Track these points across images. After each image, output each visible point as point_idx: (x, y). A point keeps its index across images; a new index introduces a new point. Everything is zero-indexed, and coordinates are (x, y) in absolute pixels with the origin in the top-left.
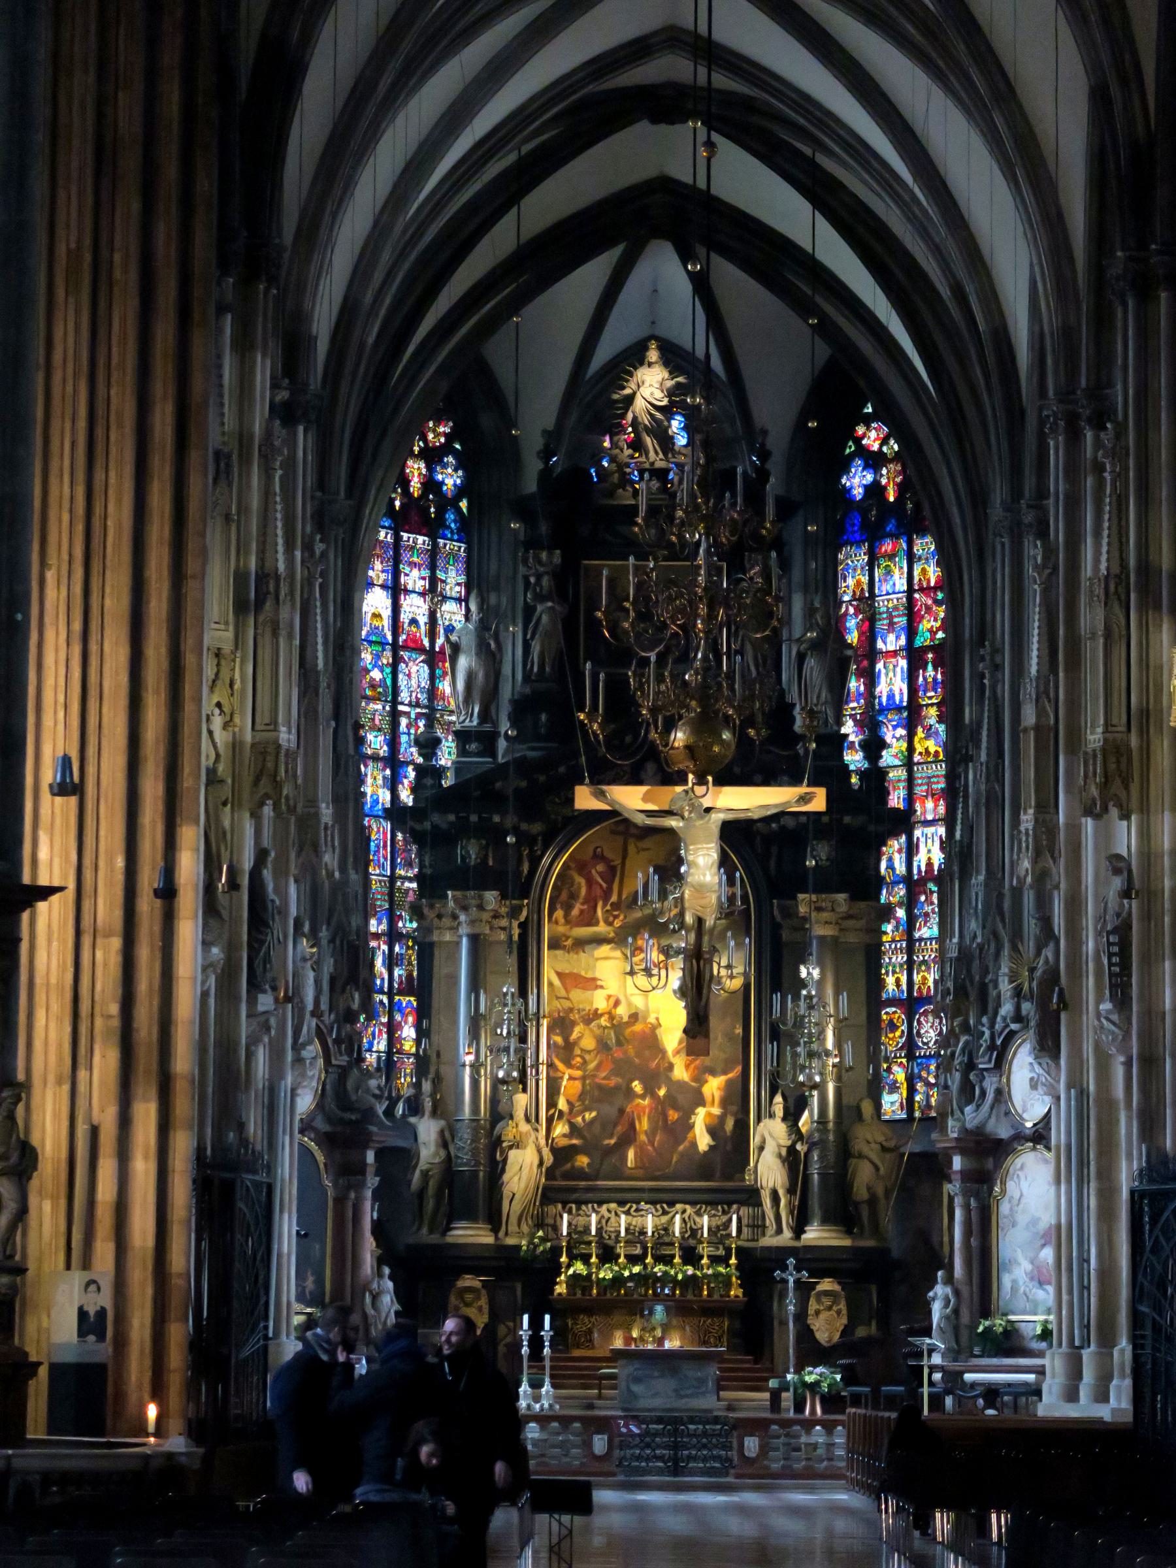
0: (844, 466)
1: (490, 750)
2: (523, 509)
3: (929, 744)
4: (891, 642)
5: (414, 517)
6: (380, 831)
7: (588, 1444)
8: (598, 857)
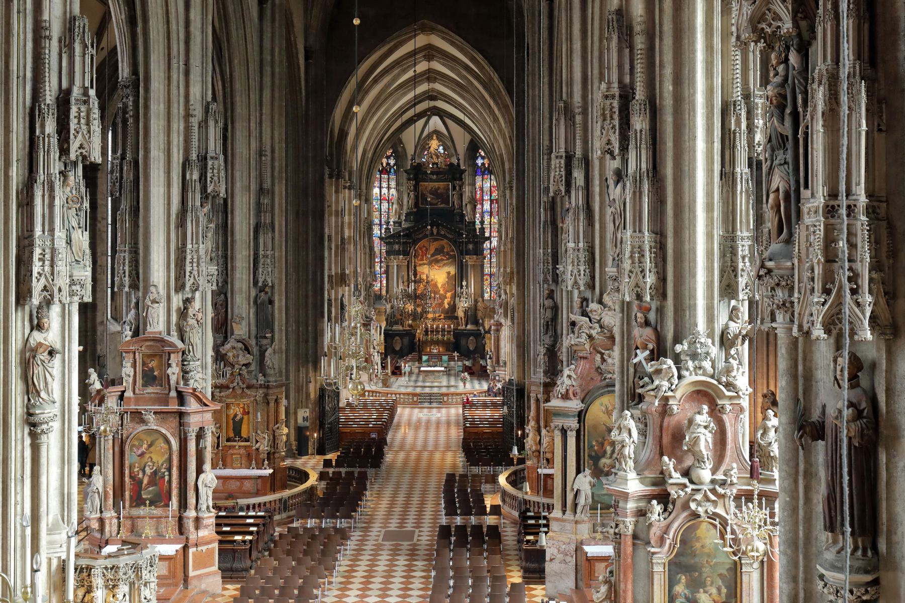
0: (477, 158)
1: (400, 226)
2: (406, 171)
3: (495, 220)
4: (486, 197)
5: (384, 171)
6: (376, 241)
7: (413, 399)
8: (424, 246)
